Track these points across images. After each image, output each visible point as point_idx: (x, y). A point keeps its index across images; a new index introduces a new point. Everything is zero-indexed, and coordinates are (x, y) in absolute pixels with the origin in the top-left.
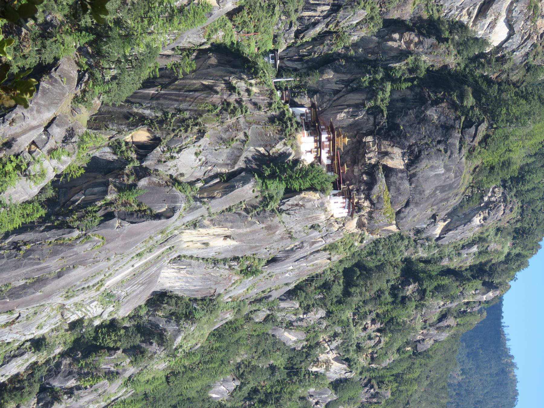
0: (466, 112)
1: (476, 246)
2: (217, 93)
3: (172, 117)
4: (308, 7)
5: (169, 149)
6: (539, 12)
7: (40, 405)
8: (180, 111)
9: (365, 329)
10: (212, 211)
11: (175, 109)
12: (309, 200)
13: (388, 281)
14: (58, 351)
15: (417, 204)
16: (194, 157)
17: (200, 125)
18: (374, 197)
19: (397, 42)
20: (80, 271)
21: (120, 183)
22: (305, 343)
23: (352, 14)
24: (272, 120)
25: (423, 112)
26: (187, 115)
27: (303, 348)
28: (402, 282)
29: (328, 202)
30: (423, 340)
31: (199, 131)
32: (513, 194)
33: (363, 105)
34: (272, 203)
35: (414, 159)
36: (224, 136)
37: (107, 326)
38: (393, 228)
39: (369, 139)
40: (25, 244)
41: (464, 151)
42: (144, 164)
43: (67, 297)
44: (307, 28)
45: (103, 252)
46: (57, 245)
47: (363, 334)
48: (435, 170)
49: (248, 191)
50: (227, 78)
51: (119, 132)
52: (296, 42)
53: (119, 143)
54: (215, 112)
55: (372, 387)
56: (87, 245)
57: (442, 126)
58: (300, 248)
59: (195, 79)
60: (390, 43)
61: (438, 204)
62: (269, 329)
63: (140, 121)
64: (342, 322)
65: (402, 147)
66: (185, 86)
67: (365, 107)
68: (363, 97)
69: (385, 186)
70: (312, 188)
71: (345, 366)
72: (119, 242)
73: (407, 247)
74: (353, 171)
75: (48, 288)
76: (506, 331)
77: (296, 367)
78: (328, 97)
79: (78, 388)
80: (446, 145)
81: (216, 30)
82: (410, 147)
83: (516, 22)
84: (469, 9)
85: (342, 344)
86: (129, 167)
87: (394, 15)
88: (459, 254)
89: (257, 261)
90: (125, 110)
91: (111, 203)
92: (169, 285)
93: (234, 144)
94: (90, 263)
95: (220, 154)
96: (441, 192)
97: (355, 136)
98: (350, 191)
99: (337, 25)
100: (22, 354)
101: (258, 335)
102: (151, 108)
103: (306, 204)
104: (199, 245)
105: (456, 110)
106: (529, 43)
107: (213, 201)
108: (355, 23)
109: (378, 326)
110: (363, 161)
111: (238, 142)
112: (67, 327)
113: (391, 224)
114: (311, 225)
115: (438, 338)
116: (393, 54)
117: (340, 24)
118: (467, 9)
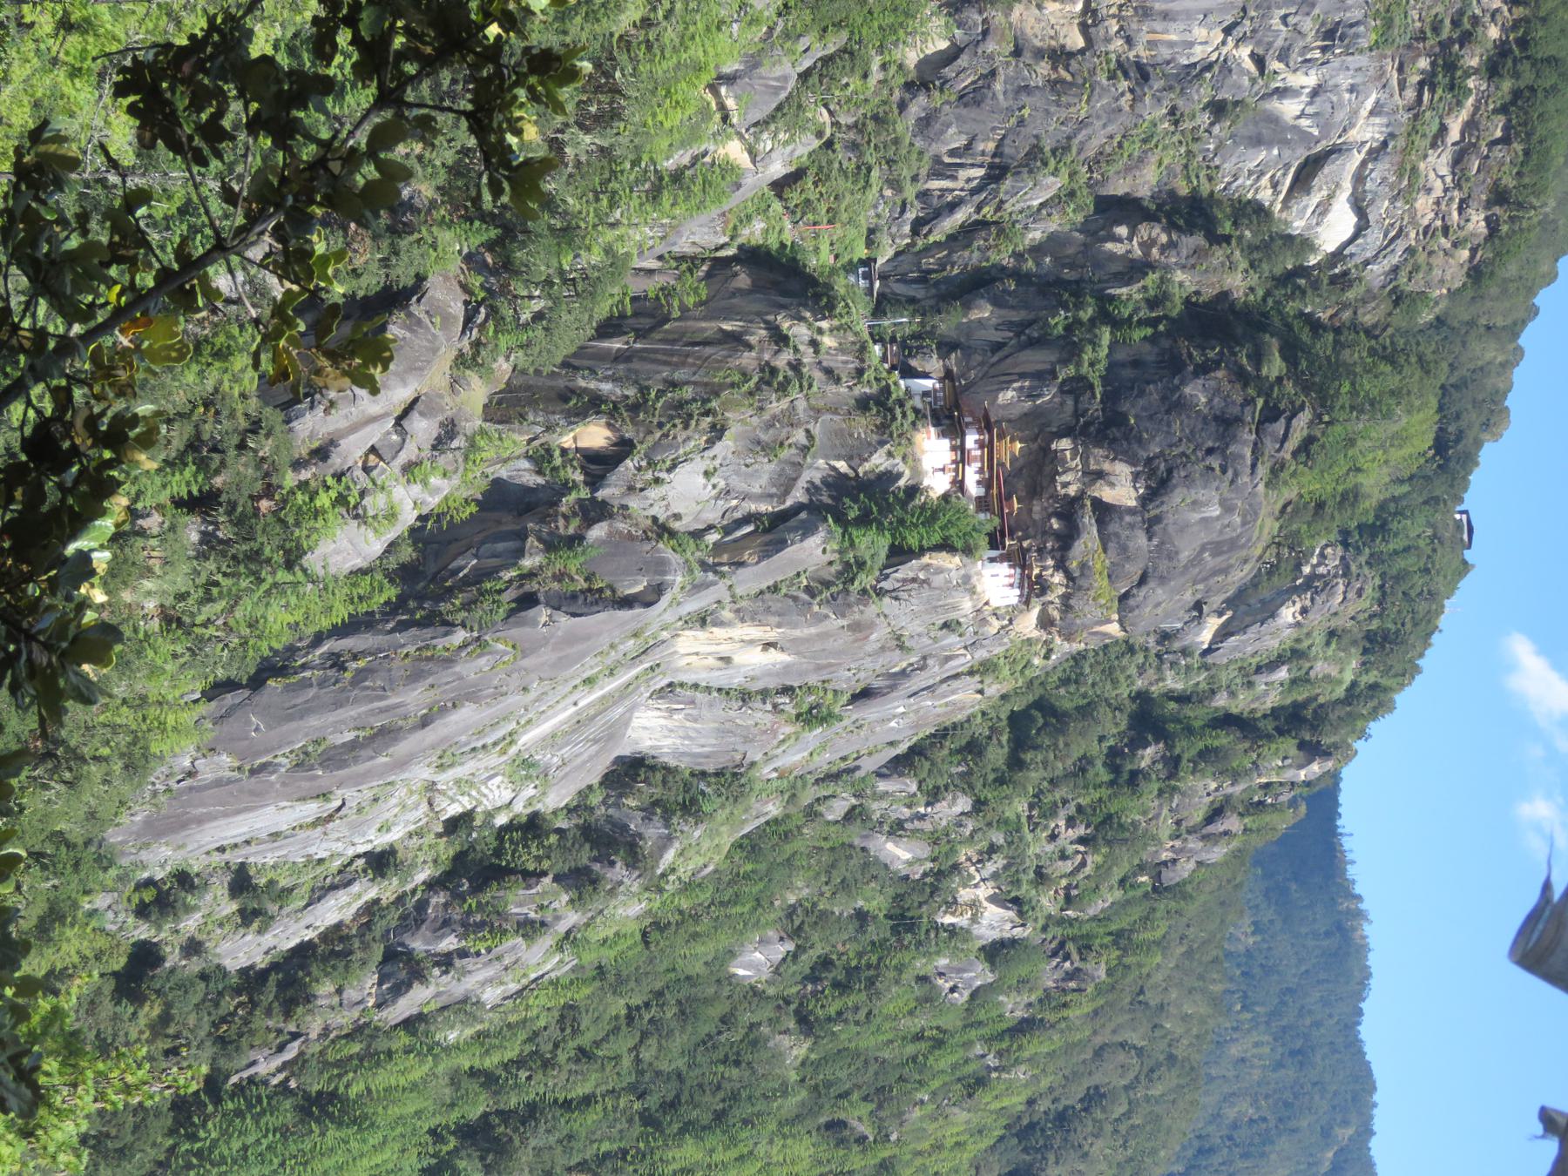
0: (1265, 388)
1: (1285, 668)
2: (750, 347)
3: (658, 397)
4: (940, 170)
5: (652, 464)
6: (1422, 181)
8: (674, 385)
9: (1053, 837)
10: (739, 591)
11: (665, 381)
12: (940, 571)
13: (1101, 739)
14: (421, 876)
15: (1163, 580)
16: (702, 480)
17: (715, 414)
18: (1073, 565)
19: (1124, 243)
20: (467, 714)
21: (551, 533)
22: (929, 865)
24: (863, 404)
25: (1178, 388)
26: (688, 392)
27: (925, 875)
28: (1132, 740)
29: (979, 574)
30: (1174, 861)
31: (713, 427)
32: (1362, 559)
34: (862, 576)
35: (1157, 485)
36: (764, 437)
37: (520, 827)
38: (1114, 629)
39: (1065, 444)
40: (355, 657)
41: (1263, 470)
42: (600, 495)
43: (441, 767)
44: (938, 214)
46: (420, 659)
47: (1050, 848)
48: (1200, 508)
49: (813, 551)
50: (771, 318)
51: (549, 428)
52: (913, 244)
53: (549, 451)
54: (745, 388)
55: (1067, 957)
56: (483, 661)
57: (1216, 418)
58: (921, 669)
59: (704, 319)
60: (1109, 246)
61: (1205, 579)
62: (854, 835)
63: (593, 405)
64: (1006, 822)
65: (1132, 462)
66: (683, 334)
68: (1053, 358)
70: (946, 546)
71: (1011, 914)
72: (547, 655)
73: (1141, 670)
74: (1030, 511)
75: (402, 748)
76: (1347, 843)
77: (911, 913)
78: (978, 358)
79: (463, 953)
80: (1225, 458)
81: (749, 218)
82: (1149, 461)
83: (1372, 201)
85: (1005, 868)
86: (568, 501)
87: (1119, 187)
88: (1250, 685)
89: (830, 695)
90: (561, 383)
91: (531, 575)
93: (785, 454)
96: (1213, 555)
97: (1035, 439)
98: (1024, 552)
99: (999, 208)
100: (349, 883)
101: (832, 849)
102: (614, 379)
104: (711, 661)
105: (1245, 386)
106: (1400, 246)
107: (741, 571)
108: (1036, 203)
109: (1081, 831)
111: (793, 451)
112: (440, 829)
113: (1109, 621)
115: (1204, 856)
116: (1115, 267)
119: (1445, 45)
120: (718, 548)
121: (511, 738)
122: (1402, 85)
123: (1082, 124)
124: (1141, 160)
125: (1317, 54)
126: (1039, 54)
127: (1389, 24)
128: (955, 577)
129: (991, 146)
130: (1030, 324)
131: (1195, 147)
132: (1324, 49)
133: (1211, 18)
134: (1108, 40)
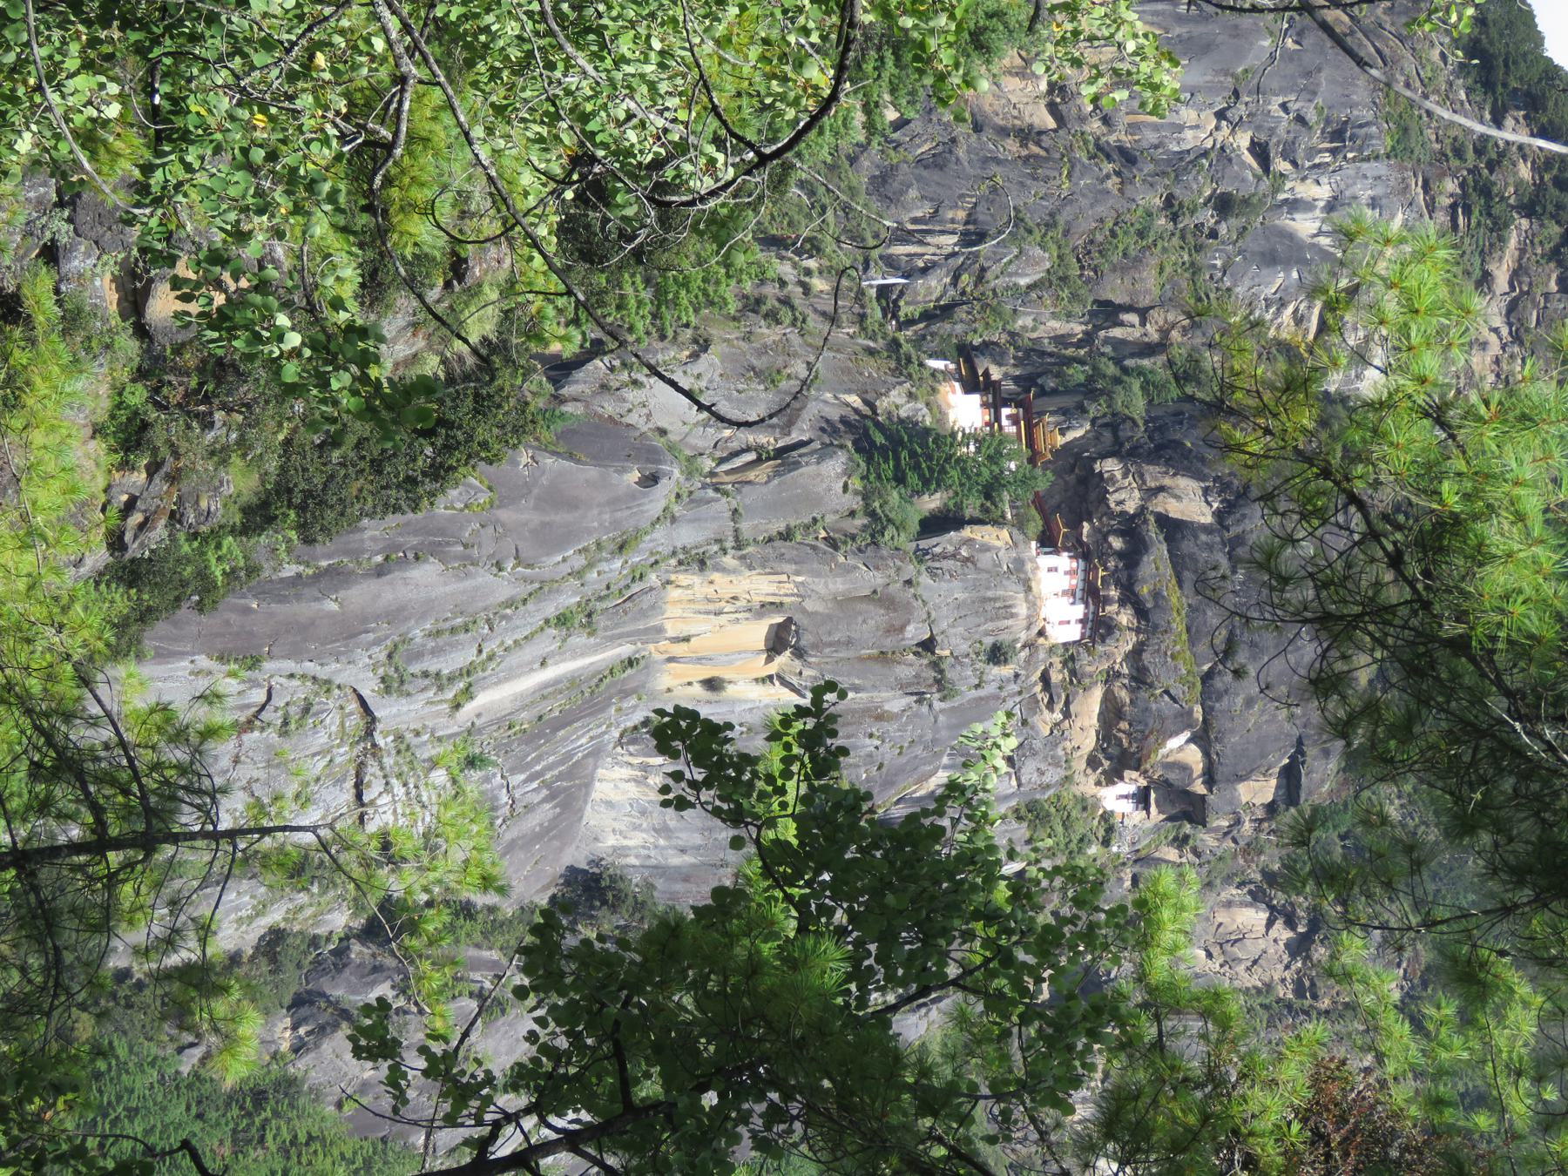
4: (903, 236)
7: (302, 1031)
10: (745, 526)
12: (986, 548)
18: (1144, 590)
23: (1016, 251)
29: (1032, 560)
33: (1083, 410)
36: (755, 362)
39: (1111, 466)
45: (490, 529)
60: (1117, 332)
65: (1200, 477)
67: (1084, 411)
69: (1169, 571)
84: (1296, 310)
92: (611, 841)
93: (783, 385)
94: (456, 558)
95: (750, 402)
97: (1072, 470)
103: (978, 556)
104: (697, 690)
107: (746, 489)
108: (1023, 282)
110: (1103, 509)
114: (989, 641)
117: (989, 275)
118: (1291, 309)
119: (1474, 171)
120: (712, 474)
121: (467, 682)
122: (1431, 207)
123: (1066, 201)
124: (1138, 260)
125: (1327, 158)
126: (1003, 132)
127: (1406, 130)
128: (1006, 558)
129: (961, 215)
130: (1040, 375)
131: (1198, 258)
132: (1333, 152)
133: (1199, 98)
134: (1082, 119)
